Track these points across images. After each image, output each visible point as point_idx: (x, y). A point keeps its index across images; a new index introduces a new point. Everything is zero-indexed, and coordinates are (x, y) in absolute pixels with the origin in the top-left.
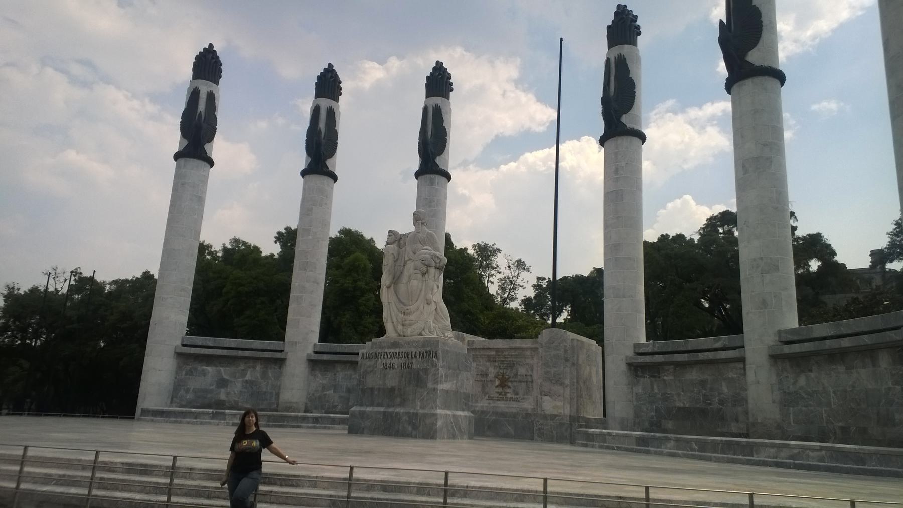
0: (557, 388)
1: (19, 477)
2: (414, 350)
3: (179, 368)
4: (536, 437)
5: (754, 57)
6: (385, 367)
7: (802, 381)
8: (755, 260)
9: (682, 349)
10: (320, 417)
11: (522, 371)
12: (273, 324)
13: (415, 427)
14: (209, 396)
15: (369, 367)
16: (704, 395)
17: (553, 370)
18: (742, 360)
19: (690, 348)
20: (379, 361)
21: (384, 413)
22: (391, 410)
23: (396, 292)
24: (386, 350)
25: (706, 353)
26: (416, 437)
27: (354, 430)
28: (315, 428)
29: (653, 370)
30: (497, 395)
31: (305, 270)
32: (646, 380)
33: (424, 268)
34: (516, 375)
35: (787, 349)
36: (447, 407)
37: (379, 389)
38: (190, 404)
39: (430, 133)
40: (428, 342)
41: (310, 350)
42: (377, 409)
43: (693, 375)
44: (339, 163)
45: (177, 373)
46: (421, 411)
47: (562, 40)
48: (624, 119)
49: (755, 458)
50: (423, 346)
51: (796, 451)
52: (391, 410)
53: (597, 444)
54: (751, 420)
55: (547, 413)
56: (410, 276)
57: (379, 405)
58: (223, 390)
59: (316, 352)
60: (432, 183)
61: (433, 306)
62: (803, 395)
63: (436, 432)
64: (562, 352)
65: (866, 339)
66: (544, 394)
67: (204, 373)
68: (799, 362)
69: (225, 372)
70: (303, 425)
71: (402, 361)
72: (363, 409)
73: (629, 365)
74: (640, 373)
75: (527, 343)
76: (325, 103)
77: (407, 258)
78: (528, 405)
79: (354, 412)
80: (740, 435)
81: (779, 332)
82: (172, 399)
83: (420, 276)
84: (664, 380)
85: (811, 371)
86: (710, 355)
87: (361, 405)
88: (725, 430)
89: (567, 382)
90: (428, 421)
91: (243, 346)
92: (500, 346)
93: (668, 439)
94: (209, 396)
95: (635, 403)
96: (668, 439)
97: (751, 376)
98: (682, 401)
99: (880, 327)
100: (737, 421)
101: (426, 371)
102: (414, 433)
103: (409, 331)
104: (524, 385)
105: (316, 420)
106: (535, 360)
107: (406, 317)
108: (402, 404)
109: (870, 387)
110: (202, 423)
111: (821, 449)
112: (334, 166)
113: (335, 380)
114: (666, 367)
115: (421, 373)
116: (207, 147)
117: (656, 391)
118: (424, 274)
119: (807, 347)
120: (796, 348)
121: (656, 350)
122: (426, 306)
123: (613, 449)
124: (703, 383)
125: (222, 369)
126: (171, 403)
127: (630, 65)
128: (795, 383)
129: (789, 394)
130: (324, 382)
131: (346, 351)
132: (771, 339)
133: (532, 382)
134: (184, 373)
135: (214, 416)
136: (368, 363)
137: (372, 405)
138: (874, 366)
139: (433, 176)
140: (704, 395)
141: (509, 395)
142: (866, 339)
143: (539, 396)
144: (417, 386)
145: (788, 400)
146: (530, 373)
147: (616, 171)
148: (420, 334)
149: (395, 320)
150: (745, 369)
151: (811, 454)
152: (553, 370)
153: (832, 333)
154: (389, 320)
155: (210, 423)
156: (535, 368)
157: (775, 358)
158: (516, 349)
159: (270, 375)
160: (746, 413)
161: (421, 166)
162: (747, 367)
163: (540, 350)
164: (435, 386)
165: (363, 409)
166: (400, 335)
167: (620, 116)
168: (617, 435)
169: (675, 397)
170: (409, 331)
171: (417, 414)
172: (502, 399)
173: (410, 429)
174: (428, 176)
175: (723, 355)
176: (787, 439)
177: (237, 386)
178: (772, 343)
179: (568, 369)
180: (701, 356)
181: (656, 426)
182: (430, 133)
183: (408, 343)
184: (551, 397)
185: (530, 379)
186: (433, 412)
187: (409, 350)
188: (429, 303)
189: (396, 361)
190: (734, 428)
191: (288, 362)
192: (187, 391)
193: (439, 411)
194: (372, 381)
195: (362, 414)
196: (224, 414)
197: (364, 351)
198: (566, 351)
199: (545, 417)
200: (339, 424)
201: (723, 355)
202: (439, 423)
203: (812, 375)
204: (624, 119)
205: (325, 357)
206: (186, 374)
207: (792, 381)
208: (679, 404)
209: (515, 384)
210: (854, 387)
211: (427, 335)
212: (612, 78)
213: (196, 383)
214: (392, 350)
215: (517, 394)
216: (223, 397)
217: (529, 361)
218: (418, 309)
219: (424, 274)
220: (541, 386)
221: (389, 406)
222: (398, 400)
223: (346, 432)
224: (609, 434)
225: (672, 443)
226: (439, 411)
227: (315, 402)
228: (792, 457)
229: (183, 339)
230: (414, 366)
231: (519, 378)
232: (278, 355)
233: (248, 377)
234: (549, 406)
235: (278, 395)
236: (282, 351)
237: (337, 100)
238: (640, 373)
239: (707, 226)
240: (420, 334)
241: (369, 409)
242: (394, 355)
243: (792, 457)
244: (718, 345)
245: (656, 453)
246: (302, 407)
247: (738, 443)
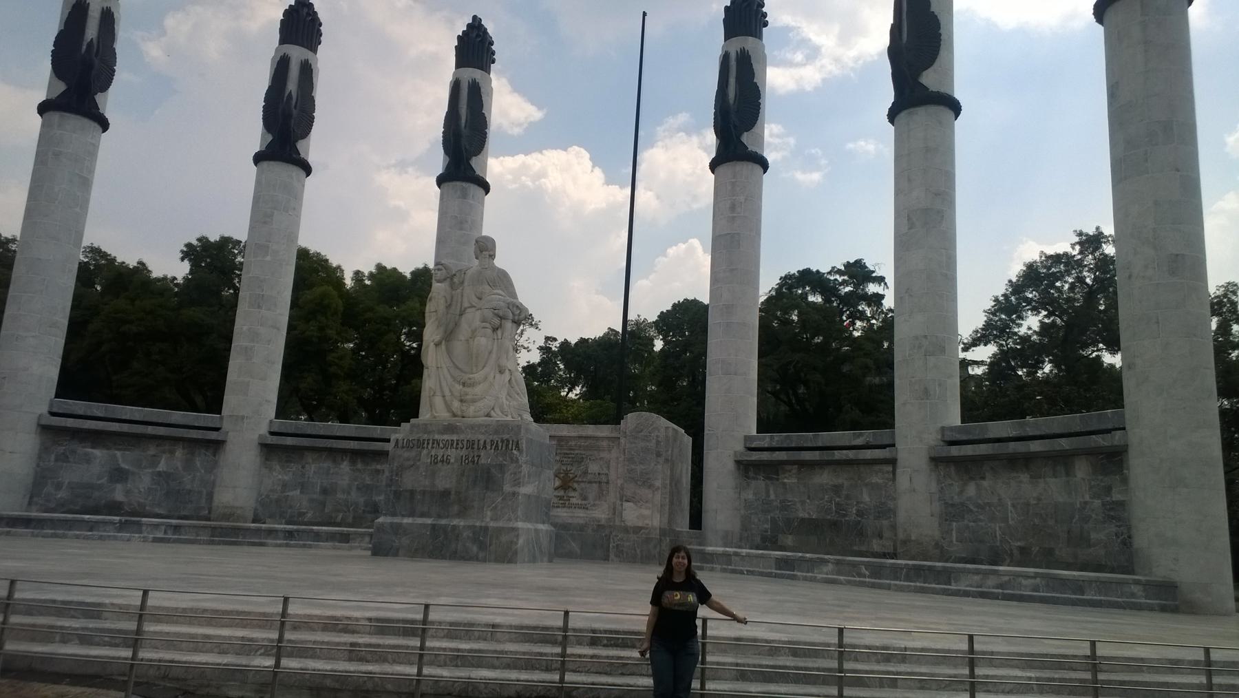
0: (645, 492)
1: (278, 650)
2: (482, 438)
3: (44, 450)
4: (612, 556)
5: (929, 79)
7: (971, 490)
8: (916, 338)
9: (810, 445)
10: (298, 531)
11: (594, 468)
12: (203, 384)
13: (482, 546)
14: (97, 494)
15: (408, 459)
16: (838, 504)
17: (639, 468)
18: (893, 462)
19: (820, 444)
20: (425, 452)
21: (433, 526)
22: (443, 522)
23: (449, 352)
24: (437, 437)
25: (845, 452)
26: (484, 560)
27: (380, 550)
28: (287, 545)
29: (770, 470)
30: (556, 500)
31: (259, 307)
32: (760, 483)
33: (497, 321)
34: (585, 473)
35: (955, 451)
36: (527, 519)
37: (424, 493)
38: (61, 507)
39: (463, 121)
40: (502, 427)
41: (264, 429)
42: (420, 521)
43: (824, 478)
44: (315, 148)
45: (40, 457)
46: (492, 524)
47: (645, 14)
48: (745, 138)
49: (953, 587)
50: (496, 432)
51: (1006, 578)
52: (443, 522)
53: (719, 567)
54: (901, 536)
55: (629, 524)
56: (474, 331)
57: (422, 515)
58: (119, 486)
59: (272, 433)
60: (464, 196)
61: (507, 376)
62: (972, 507)
63: (516, 553)
64: (652, 444)
65: (1064, 444)
66: (624, 498)
67: (88, 460)
68: (968, 467)
69: (123, 458)
70: (269, 541)
71: (464, 452)
72: (397, 520)
73: (738, 463)
74: (751, 474)
75: (604, 431)
76: (297, 53)
77: (466, 304)
78: (600, 513)
79: (382, 524)
80: (884, 556)
81: (943, 429)
82: (31, 497)
83: (489, 331)
84: (784, 484)
85: (983, 478)
86: (851, 454)
87: (394, 515)
88: (864, 548)
89: (658, 483)
90: (504, 538)
91: (154, 420)
92: (565, 433)
93: (827, 561)
94: (97, 494)
95: (742, 512)
96: (827, 561)
97: (903, 481)
98: (807, 511)
99: (1078, 429)
100: (880, 536)
101: (501, 468)
102: (481, 555)
103: (471, 410)
104: (595, 486)
105: (290, 535)
106: (614, 453)
107: (466, 389)
108: (462, 514)
109: (1061, 500)
110: (101, 538)
111: (1036, 575)
112: (307, 154)
113: (303, 475)
114: (788, 467)
115: (493, 470)
116: (99, 97)
117: (772, 497)
118: (495, 330)
119: (983, 449)
120: (968, 450)
121: (774, 444)
122: (498, 376)
123: (741, 572)
124: (837, 489)
125: (118, 454)
126: (30, 504)
127: (755, 66)
128: (961, 492)
129: (953, 505)
130: (286, 478)
131: (322, 433)
132: (932, 438)
133: (607, 483)
134: (53, 457)
135: (122, 527)
136: (406, 455)
137: (412, 514)
138: (1068, 474)
139: (464, 184)
140: (838, 504)
141: (574, 501)
142: (1064, 444)
143: (618, 502)
144: (487, 488)
145: (952, 512)
146: (605, 471)
147: (733, 208)
148: (488, 415)
149: (447, 393)
150: (894, 472)
151: (1024, 582)
152: (639, 468)
153: (1013, 434)
154: (438, 393)
155: (115, 538)
156: (613, 464)
157: (936, 461)
158: (587, 438)
159: (198, 464)
160: (894, 527)
161: (448, 168)
162: (899, 471)
163: (622, 441)
164: (516, 489)
165: (397, 520)
166: (455, 415)
167: (741, 134)
168: (748, 555)
169: (798, 505)
170: (471, 410)
171: (486, 528)
172: (564, 506)
173: (475, 549)
174: (458, 183)
175: (869, 454)
176: (946, 561)
177: (144, 481)
178: (933, 443)
179: (660, 467)
180: (838, 455)
181: (769, 541)
182: (463, 121)
183: (472, 427)
184: (635, 503)
185: (604, 479)
186: (511, 525)
187: (475, 437)
188: (501, 372)
189: (452, 453)
190: (876, 546)
191: (229, 447)
192: (59, 486)
193: (520, 525)
194: (409, 481)
195: (396, 529)
196: (139, 524)
197: (399, 436)
198: (658, 443)
199: (626, 530)
200: (327, 541)
201: (869, 454)
202: (521, 541)
203: (985, 483)
204: (745, 138)
205: (289, 441)
206: (56, 460)
207: (957, 490)
208: (802, 515)
209: (583, 485)
210: (1039, 499)
211: (498, 416)
212: (732, 81)
213: (73, 474)
214: (446, 437)
215: (585, 499)
216: (119, 496)
217: (604, 455)
218: (486, 378)
219: (495, 330)
220: (622, 489)
221: (439, 516)
222: (456, 508)
223: (369, 553)
224: (736, 554)
225: (830, 567)
226: (520, 525)
227: (269, 508)
228: (1001, 586)
229: (51, 405)
230: (483, 461)
231: (589, 477)
232: (213, 435)
233: (162, 467)
234: (632, 514)
235: (210, 496)
236: (217, 429)
237: (315, 51)
238: (751, 474)
239: (781, 286)
240: (488, 415)
241: (407, 521)
243: (1001, 586)
244: (859, 442)
245: (805, 579)
246: (250, 515)
247: (930, 568)
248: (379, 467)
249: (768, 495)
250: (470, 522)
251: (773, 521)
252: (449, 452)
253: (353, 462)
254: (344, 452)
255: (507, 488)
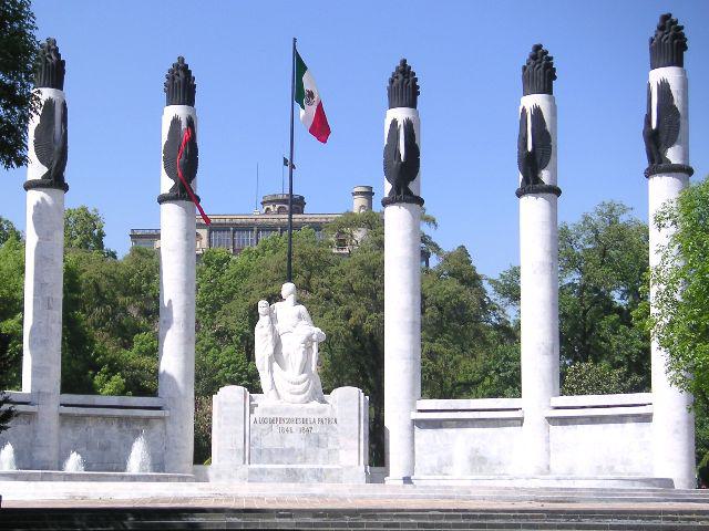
2: (312, 417)
6: (282, 430)
15: (263, 430)
46: (324, 467)
48: (412, 186)
57: (277, 463)
72: (262, 466)
108: (305, 460)
137: (271, 461)
165: (262, 466)
171: (322, 469)
204: (412, 186)
214: (287, 416)
241: (269, 466)
242: (290, 421)
248: (138, 428)
249: (435, 441)
250: (312, 466)
251: (440, 459)
252: (291, 425)
253: (120, 426)
254: (113, 417)
255: (330, 446)
